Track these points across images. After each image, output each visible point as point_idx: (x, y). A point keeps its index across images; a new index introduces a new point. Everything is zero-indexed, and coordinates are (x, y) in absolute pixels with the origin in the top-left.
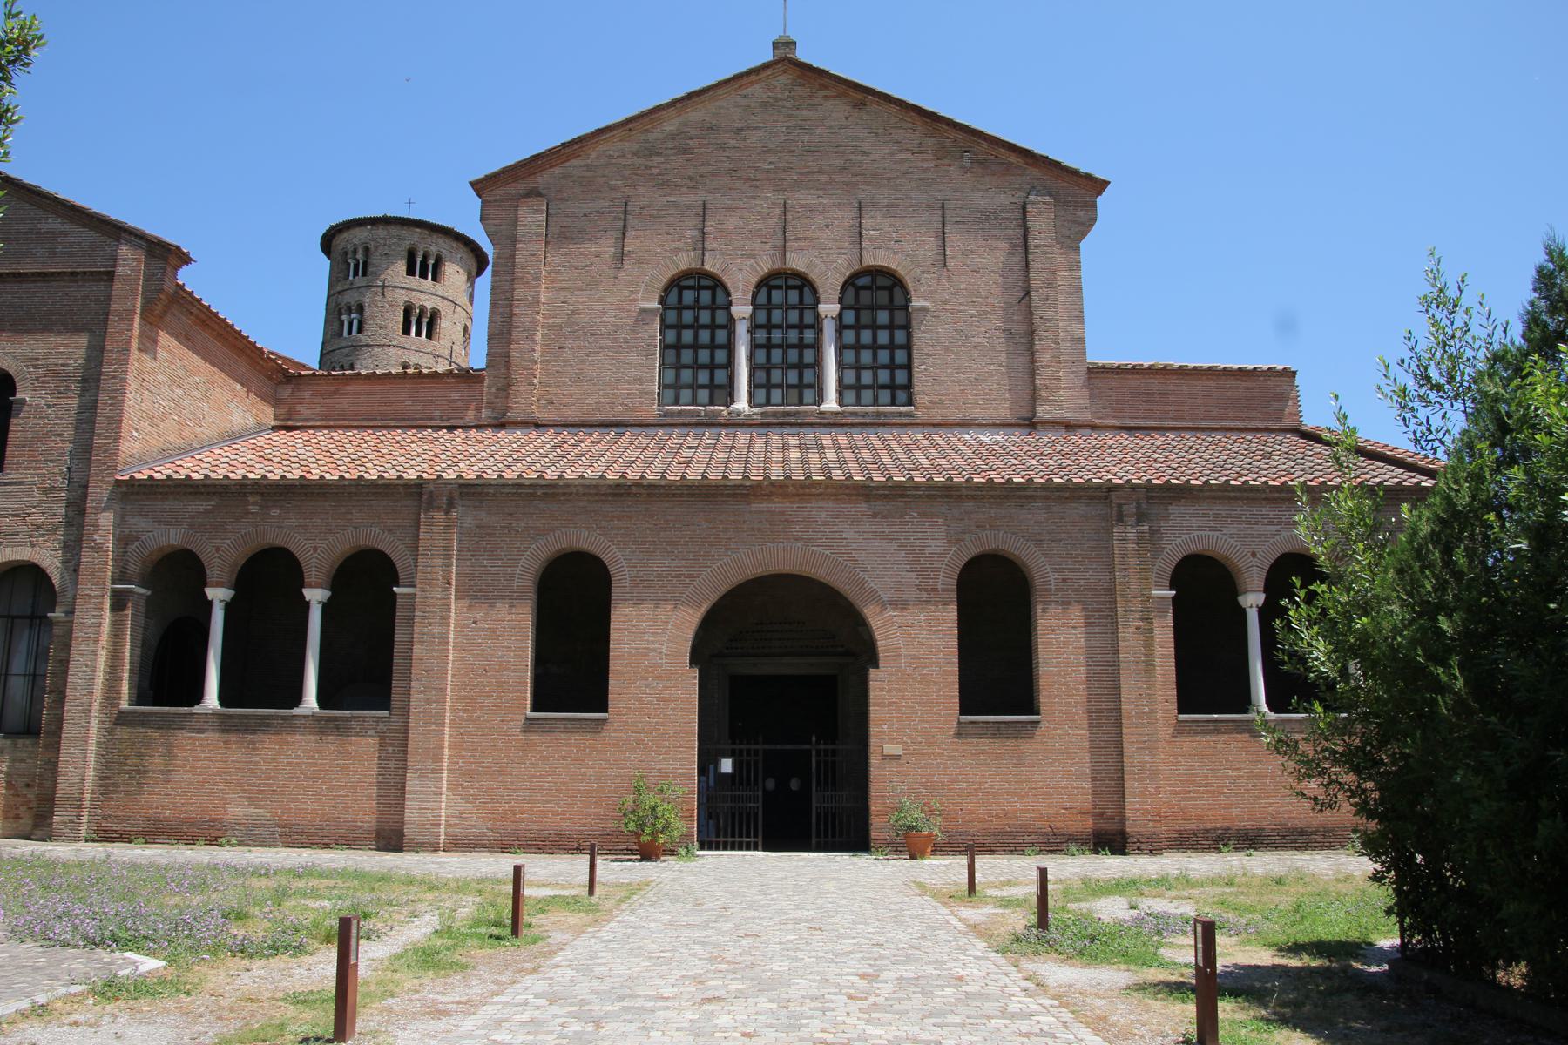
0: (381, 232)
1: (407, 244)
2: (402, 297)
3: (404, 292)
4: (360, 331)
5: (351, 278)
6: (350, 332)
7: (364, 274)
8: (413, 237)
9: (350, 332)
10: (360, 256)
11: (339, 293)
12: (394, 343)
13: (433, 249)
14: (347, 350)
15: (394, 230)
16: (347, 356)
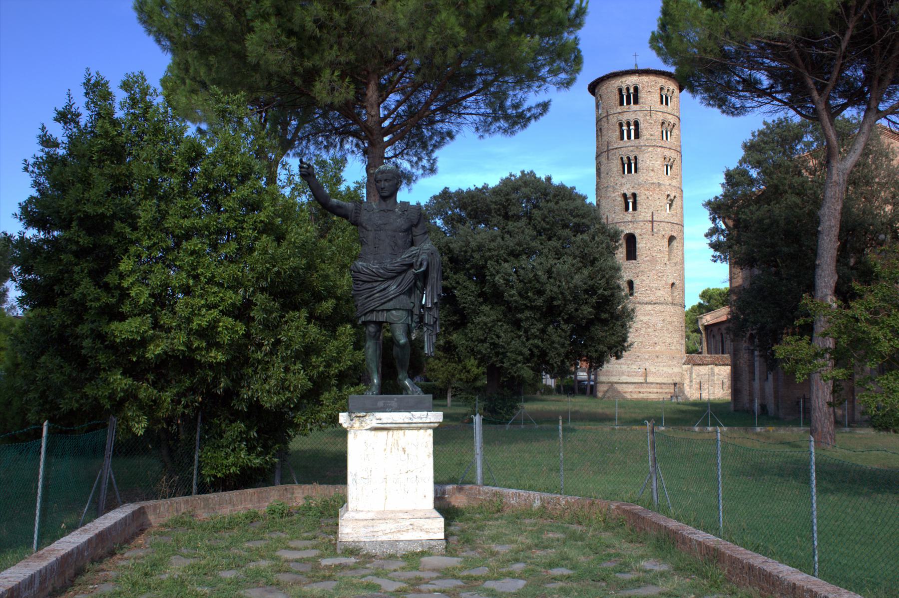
0: (645, 79)
1: (659, 86)
2: (660, 117)
3: (660, 114)
4: (637, 136)
5: (625, 104)
6: (629, 137)
7: (636, 102)
8: (662, 81)
9: (629, 137)
10: (632, 91)
11: (620, 113)
12: (660, 145)
13: (671, 88)
14: (631, 148)
15: (652, 78)
16: (632, 151)
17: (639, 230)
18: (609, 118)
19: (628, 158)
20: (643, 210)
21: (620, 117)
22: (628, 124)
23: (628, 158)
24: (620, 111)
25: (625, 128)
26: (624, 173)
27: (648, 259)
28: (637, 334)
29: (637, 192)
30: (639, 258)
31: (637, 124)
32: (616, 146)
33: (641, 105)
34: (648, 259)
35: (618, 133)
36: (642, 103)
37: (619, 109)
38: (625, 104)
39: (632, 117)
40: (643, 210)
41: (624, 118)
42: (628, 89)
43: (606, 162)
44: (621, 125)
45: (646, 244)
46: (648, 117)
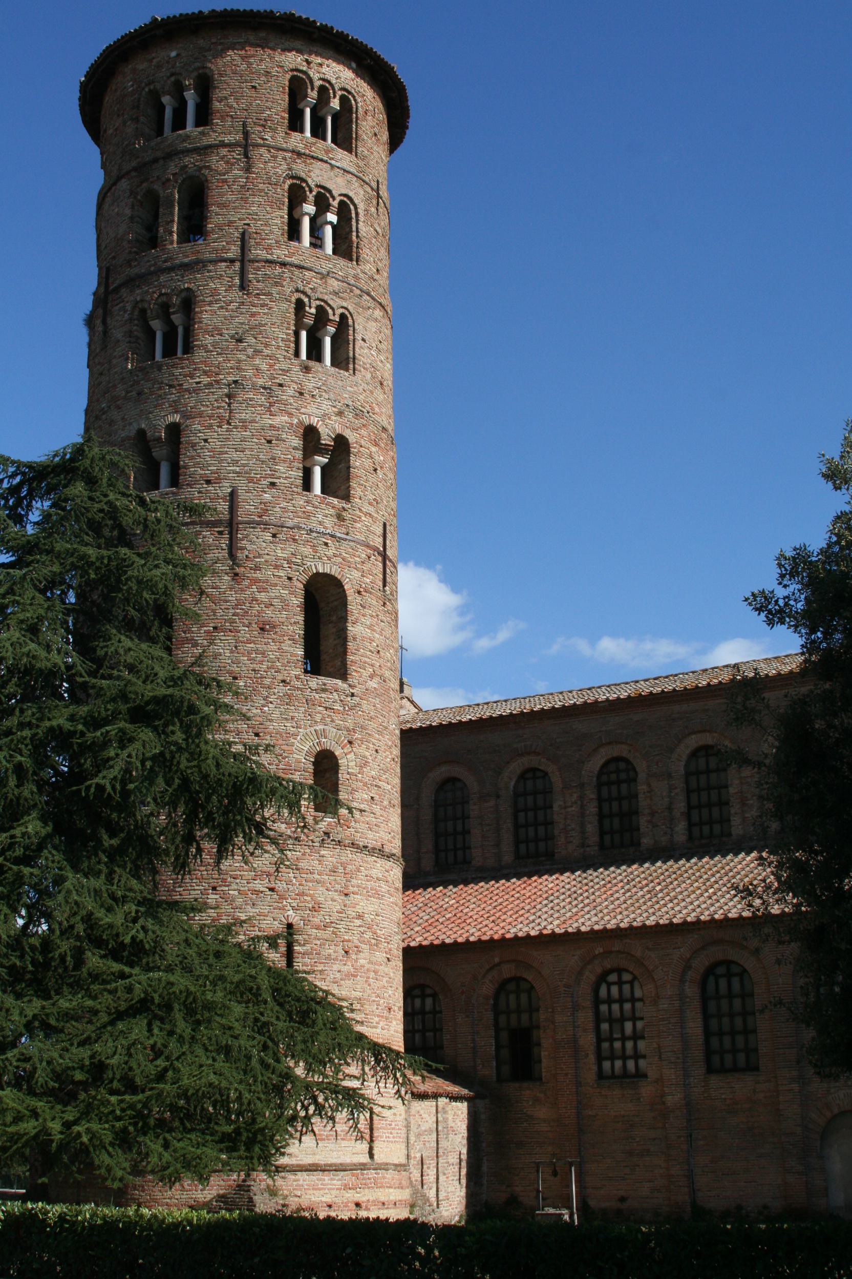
10: (335, 104)
11: (299, 154)
14: (334, 284)
16: (336, 293)
17: (356, 574)
18: (254, 153)
19: (321, 313)
20: (367, 508)
21: (300, 168)
22: (322, 203)
23: (321, 311)
24: (301, 148)
25: (309, 208)
26: (297, 354)
27: (373, 684)
28: (348, 968)
29: (351, 436)
30: (355, 676)
31: (344, 210)
32: (280, 253)
33: (361, 163)
34: (373, 684)
35: (280, 217)
36: (364, 158)
37: (296, 140)
38: (308, 133)
39: (338, 186)
40: (367, 508)
41: (317, 175)
42: (324, 92)
43: (236, 294)
44: (296, 196)
45: (371, 627)
46: (373, 210)
